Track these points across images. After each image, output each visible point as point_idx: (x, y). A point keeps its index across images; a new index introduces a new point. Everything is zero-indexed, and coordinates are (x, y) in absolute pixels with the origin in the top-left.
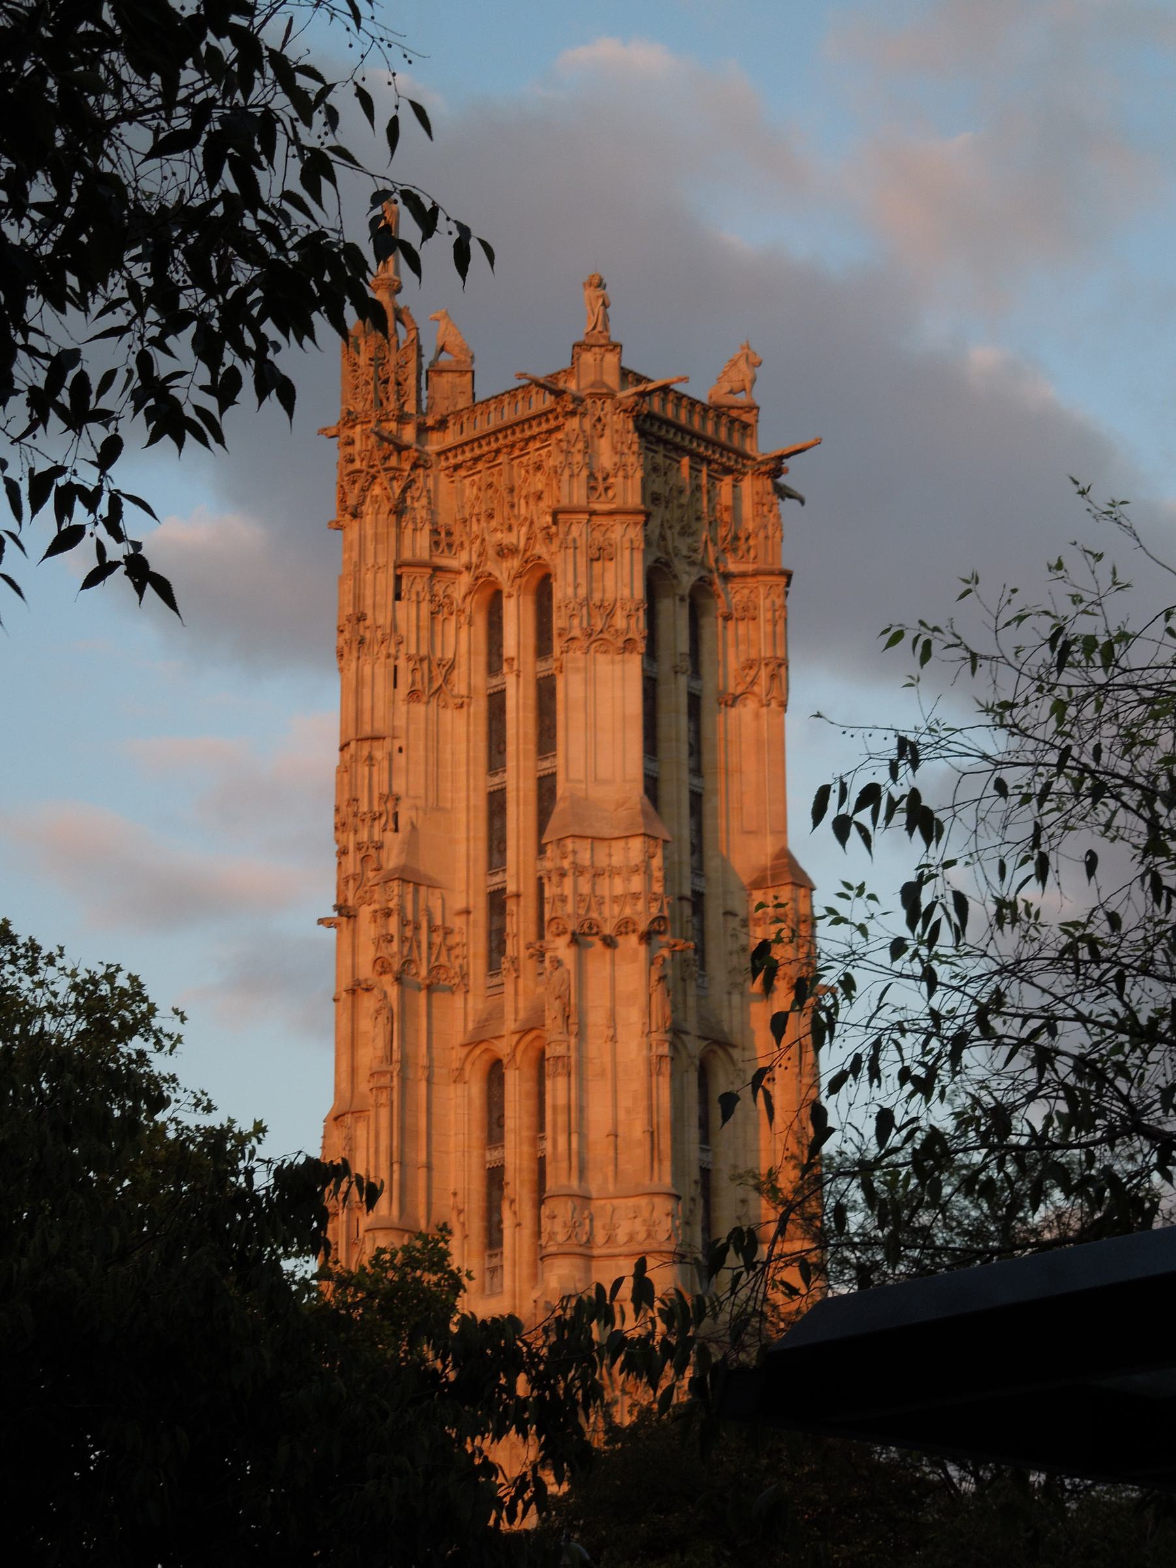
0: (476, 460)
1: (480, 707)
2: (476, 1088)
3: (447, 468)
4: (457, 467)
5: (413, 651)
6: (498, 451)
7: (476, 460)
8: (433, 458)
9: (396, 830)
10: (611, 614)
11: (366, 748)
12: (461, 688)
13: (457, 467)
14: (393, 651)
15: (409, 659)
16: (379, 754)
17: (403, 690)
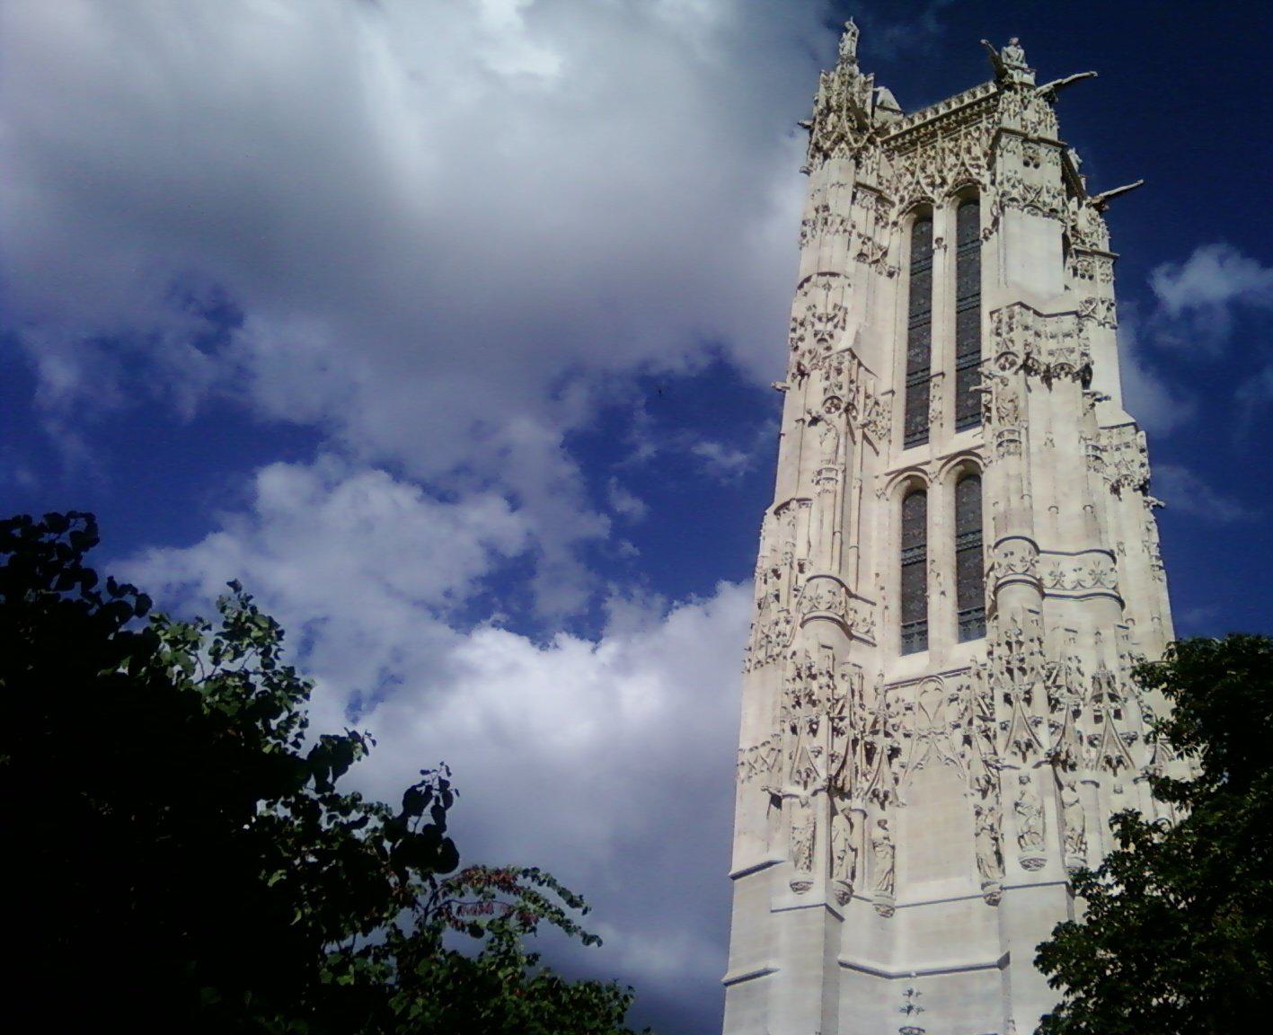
0: (913, 143)
1: (905, 277)
2: (895, 506)
3: (888, 150)
4: (898, 149)
5: (862, 232)
6: (934, 135)
7: (913, 143)
8: (879, 144)
9: (843, 328)
10: (1038, 193)
11: (824, 280)
12: (891, 260)
13: (898, 149)
14: (849, 228)
15: (860, 236)
16: (834, 285)
17: (854, 252)
